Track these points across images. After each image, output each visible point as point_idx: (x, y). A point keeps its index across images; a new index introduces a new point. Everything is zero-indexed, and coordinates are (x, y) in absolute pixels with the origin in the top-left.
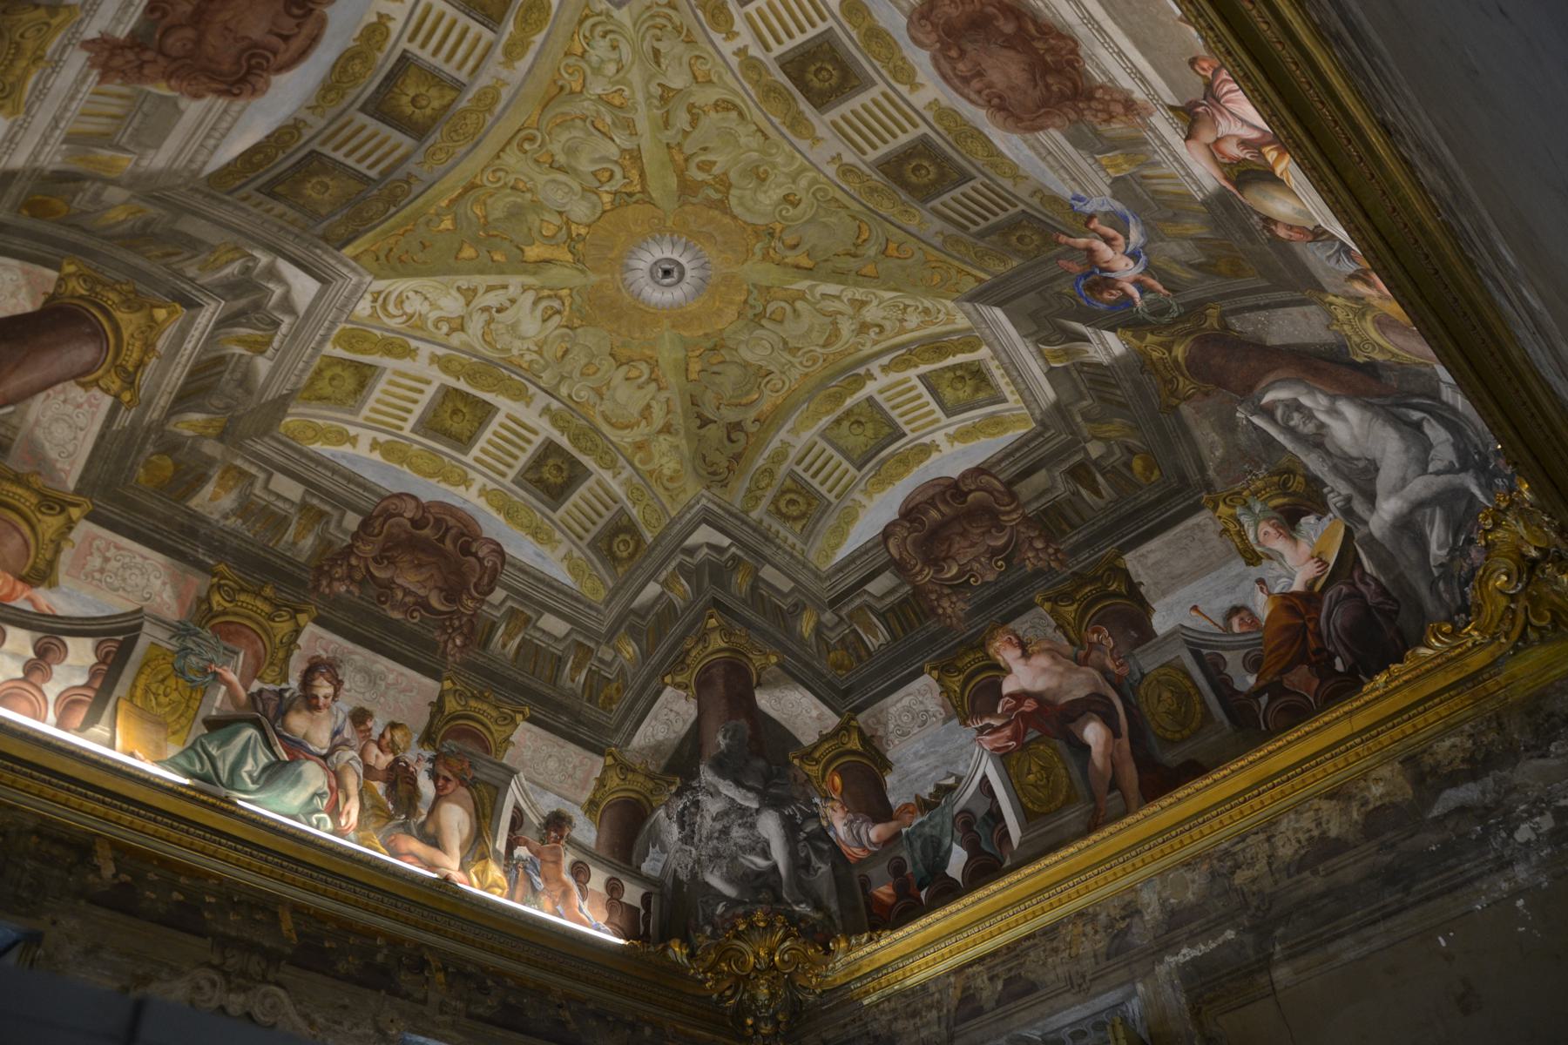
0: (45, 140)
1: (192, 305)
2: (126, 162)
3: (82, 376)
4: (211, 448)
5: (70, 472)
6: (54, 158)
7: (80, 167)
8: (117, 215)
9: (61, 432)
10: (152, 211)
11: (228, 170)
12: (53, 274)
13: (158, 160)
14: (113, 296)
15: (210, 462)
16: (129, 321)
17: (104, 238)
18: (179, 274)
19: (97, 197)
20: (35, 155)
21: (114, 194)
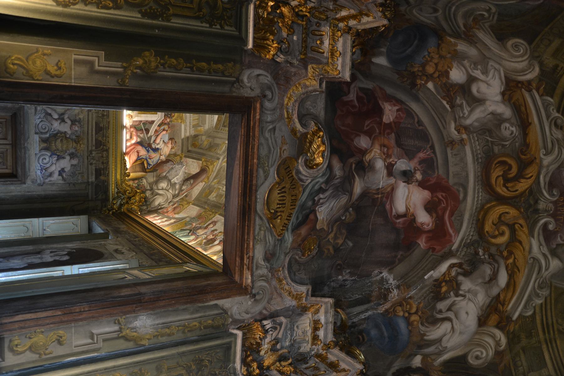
0: (190, 129)
1: (218, 159)
2: (202, 129)
3: (202, 182)
4: (216, 186)
5: (194, 197)
6: (193, 133)
7: (196, 133)
8: (205, 143)
9: (196, 191)
10: (210, 140)
11: (217, 124)
12: (201, 162)
13: (207, 127)
14: (209, 163)
15: (215, 188)
16: (211, 167)
17: (206, 150)
18: (217, 154)
19: (201, 140)
20: (190, 132)
21: (204, 138)
